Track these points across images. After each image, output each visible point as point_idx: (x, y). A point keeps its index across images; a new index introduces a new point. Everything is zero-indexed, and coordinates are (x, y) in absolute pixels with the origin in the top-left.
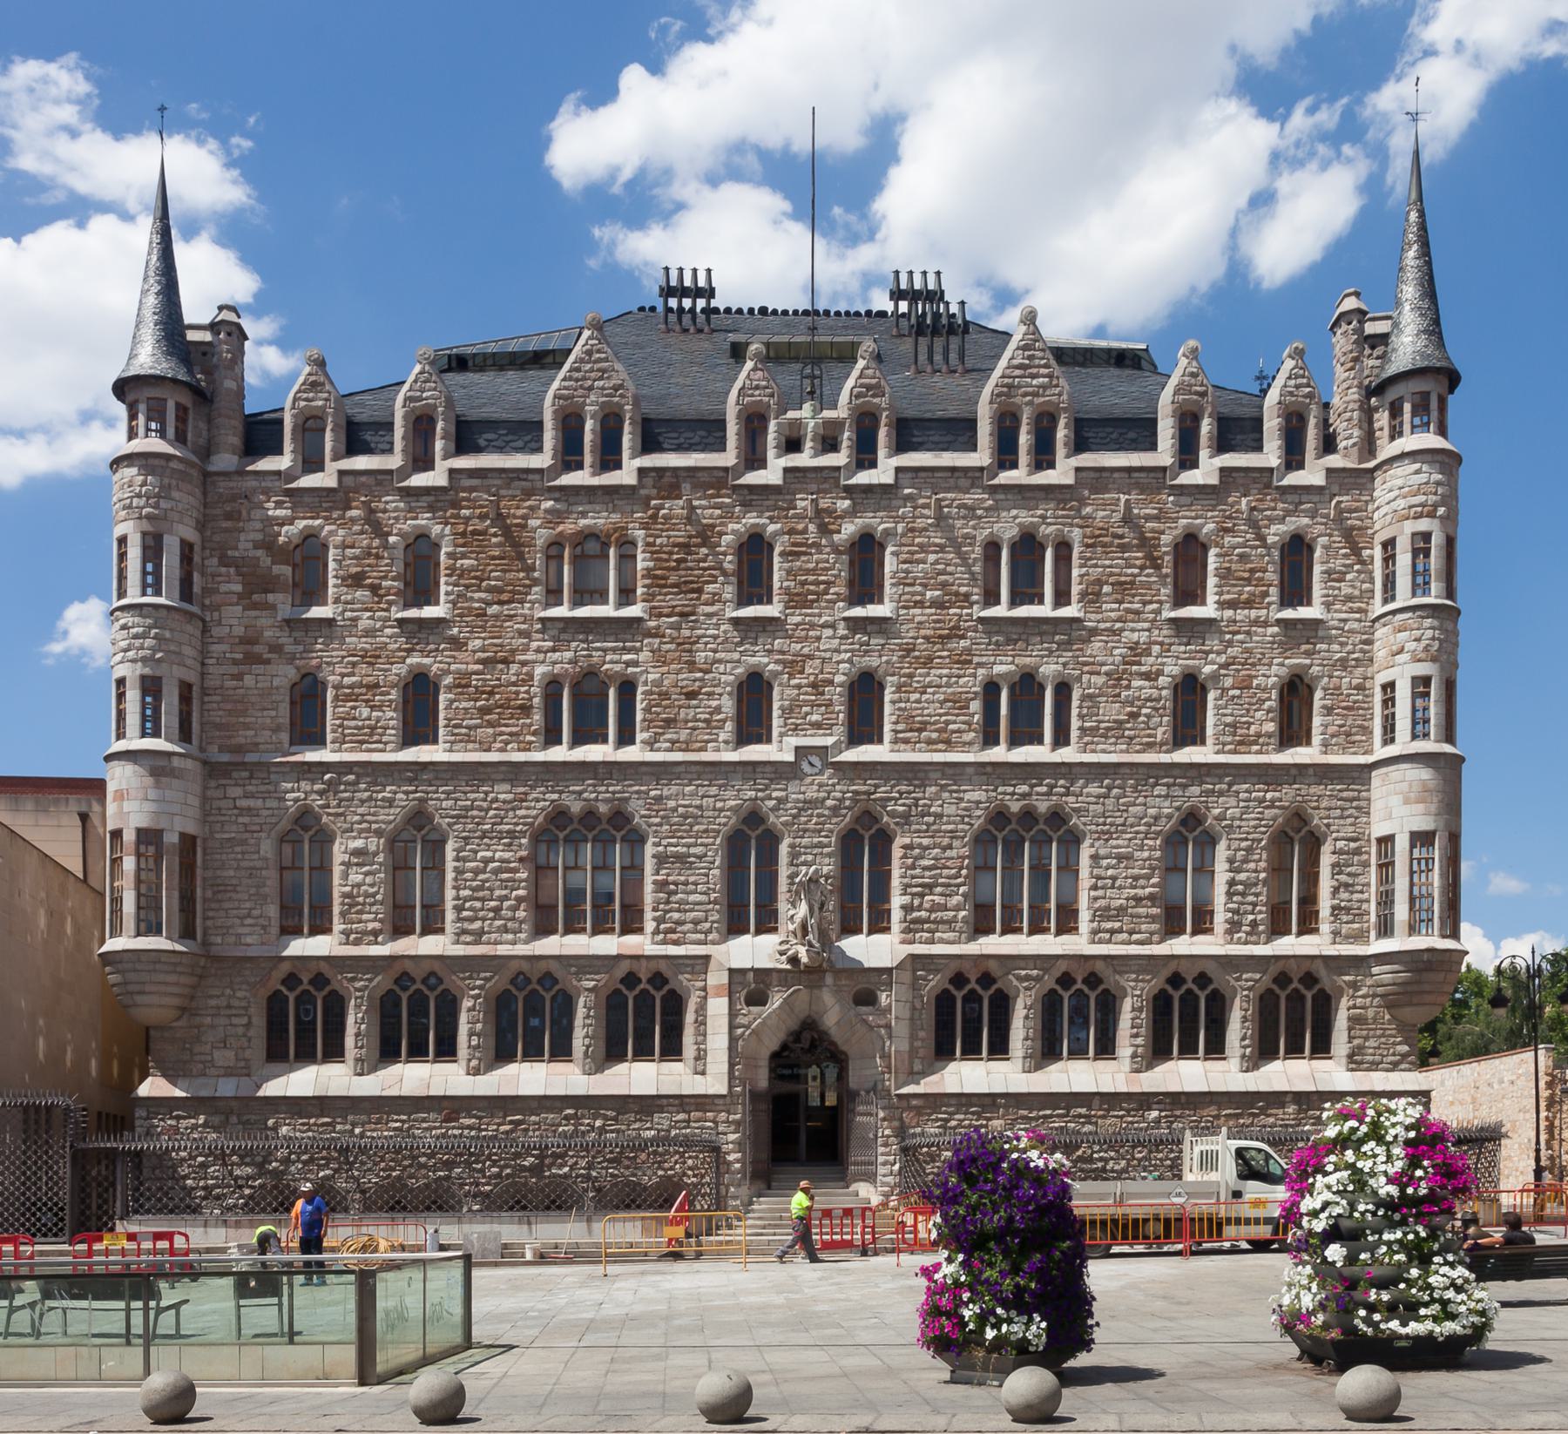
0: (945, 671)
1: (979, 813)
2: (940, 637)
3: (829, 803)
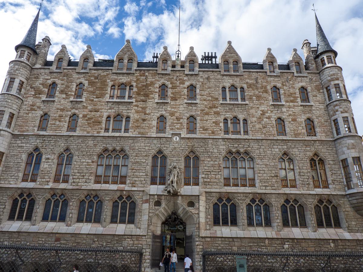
0: (214, 116)
1: (223, 152)
2: (211, 108)
3: (180, 148)
